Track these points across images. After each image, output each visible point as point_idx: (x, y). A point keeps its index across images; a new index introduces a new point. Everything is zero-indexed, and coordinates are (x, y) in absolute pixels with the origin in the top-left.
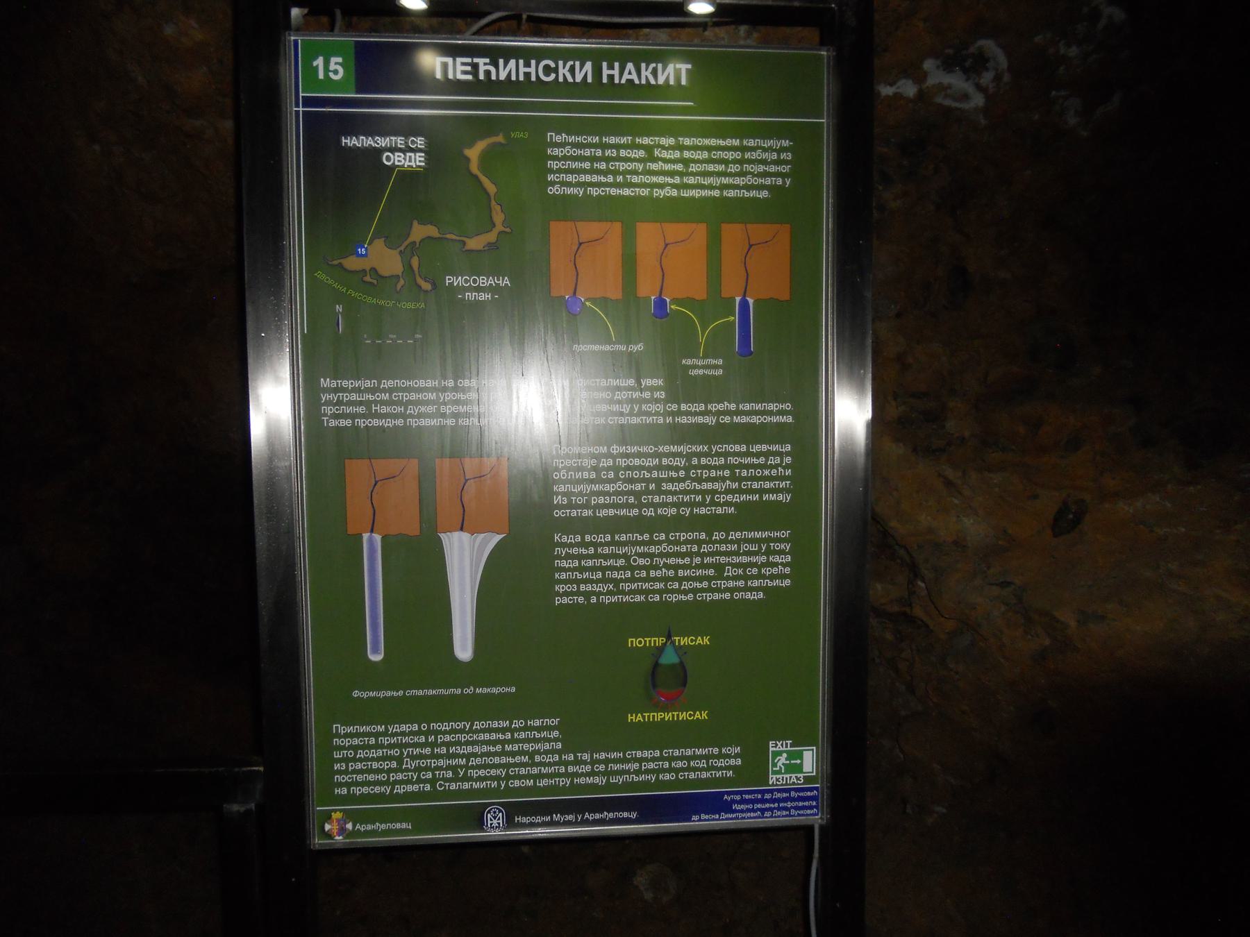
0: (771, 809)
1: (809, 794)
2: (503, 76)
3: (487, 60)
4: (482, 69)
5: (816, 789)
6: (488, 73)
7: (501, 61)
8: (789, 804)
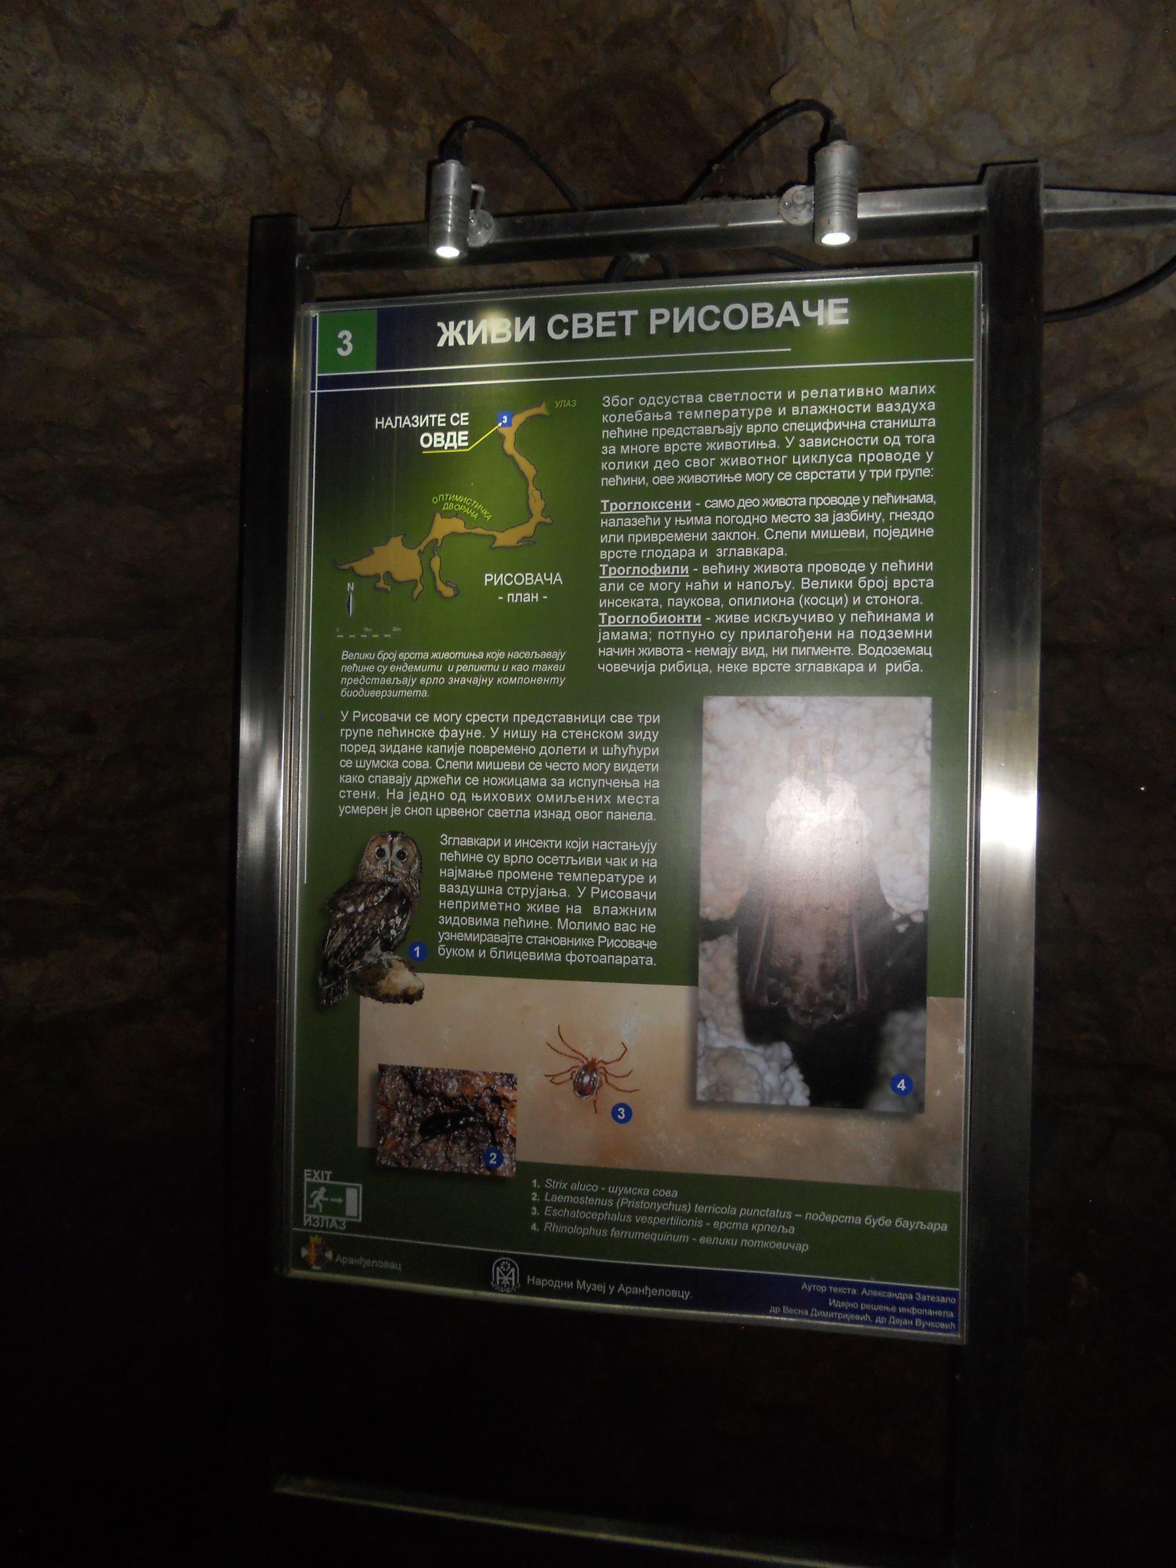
0: (886, 1314)
8: (913, 1311)
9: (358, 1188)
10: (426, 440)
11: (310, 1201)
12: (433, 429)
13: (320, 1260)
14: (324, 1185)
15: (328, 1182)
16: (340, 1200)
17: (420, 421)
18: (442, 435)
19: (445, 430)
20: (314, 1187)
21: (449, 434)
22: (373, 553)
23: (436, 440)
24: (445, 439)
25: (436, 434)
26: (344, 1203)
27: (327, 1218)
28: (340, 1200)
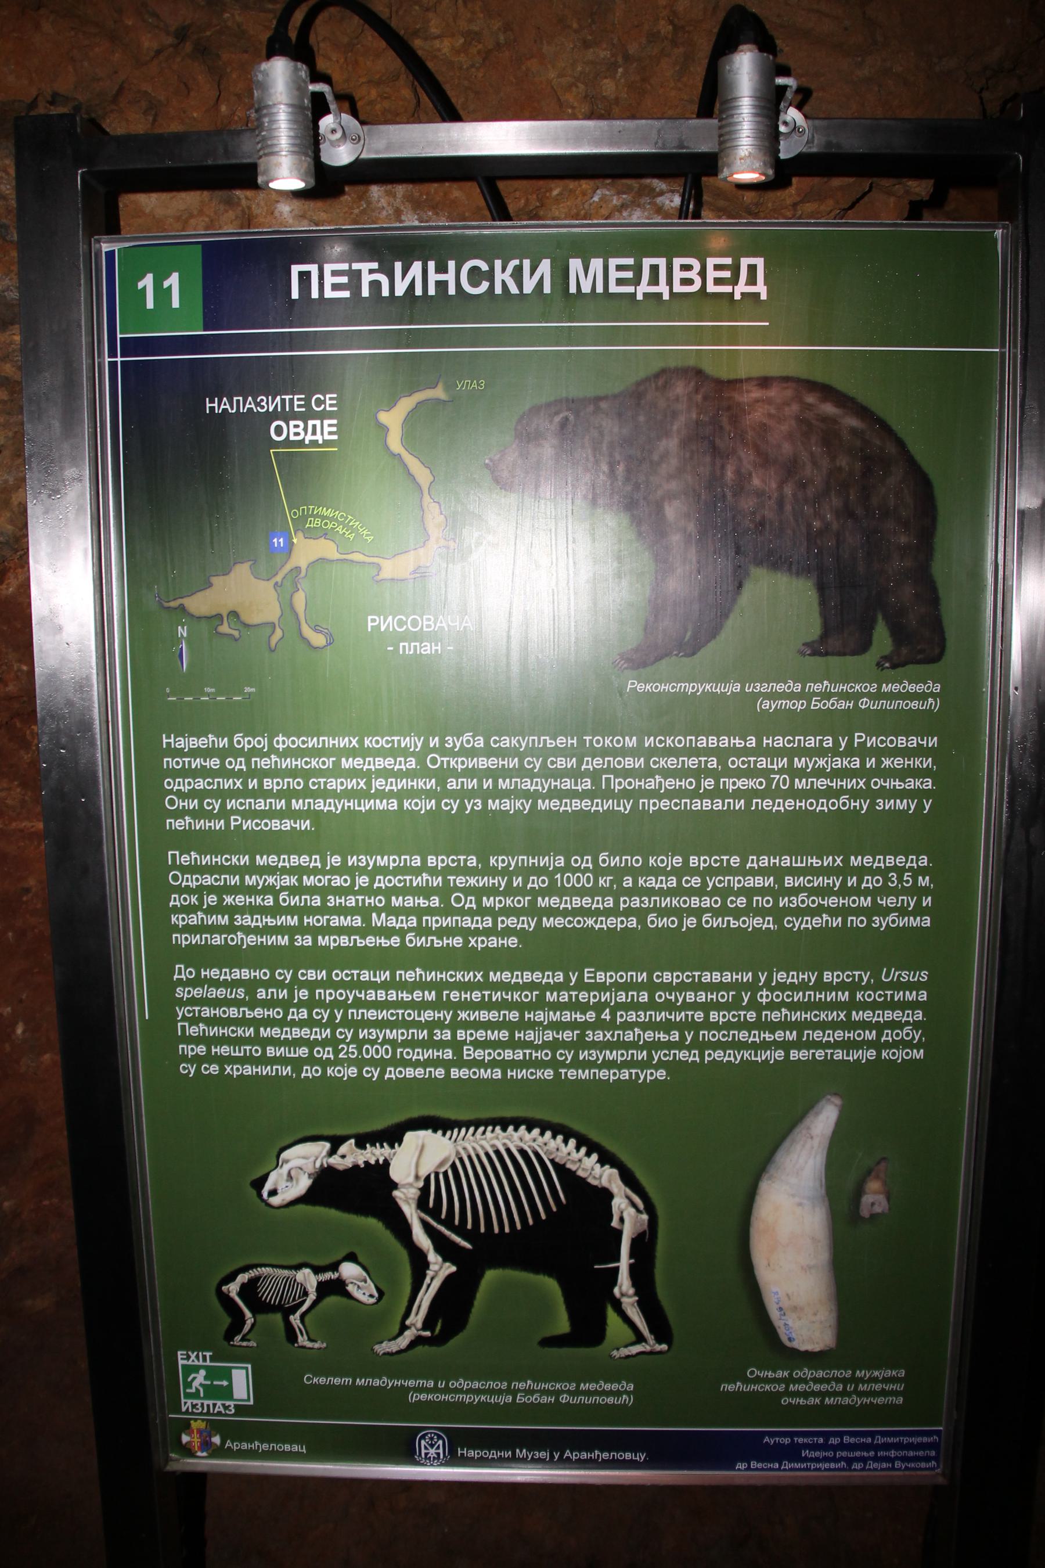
0: (864, 1460)
1: (925, 1439)
2: (400, 290)
3: (375, 265)
4: (366, 279)
5: (938, 1433)
6: (375, 285)
7: (398, 266)
9: (247, 1369)
10: (279, 431)
11: (188, 1385)
12: (287, 416)
13: (206, 1445)
14: (206, 1368)
15: (208, 1363)
16: (225, 1383)
17: (269, 404)
18: (300, 423)
19: (305, 417)
20: (190, 1370)
21: (311, 423)
22: (211, 585)
23: (292, 430)
24: (305, 429)
25: (292, 423)
26: (230, 1386)
27: (211, 1402)
28: (225, 1383)
